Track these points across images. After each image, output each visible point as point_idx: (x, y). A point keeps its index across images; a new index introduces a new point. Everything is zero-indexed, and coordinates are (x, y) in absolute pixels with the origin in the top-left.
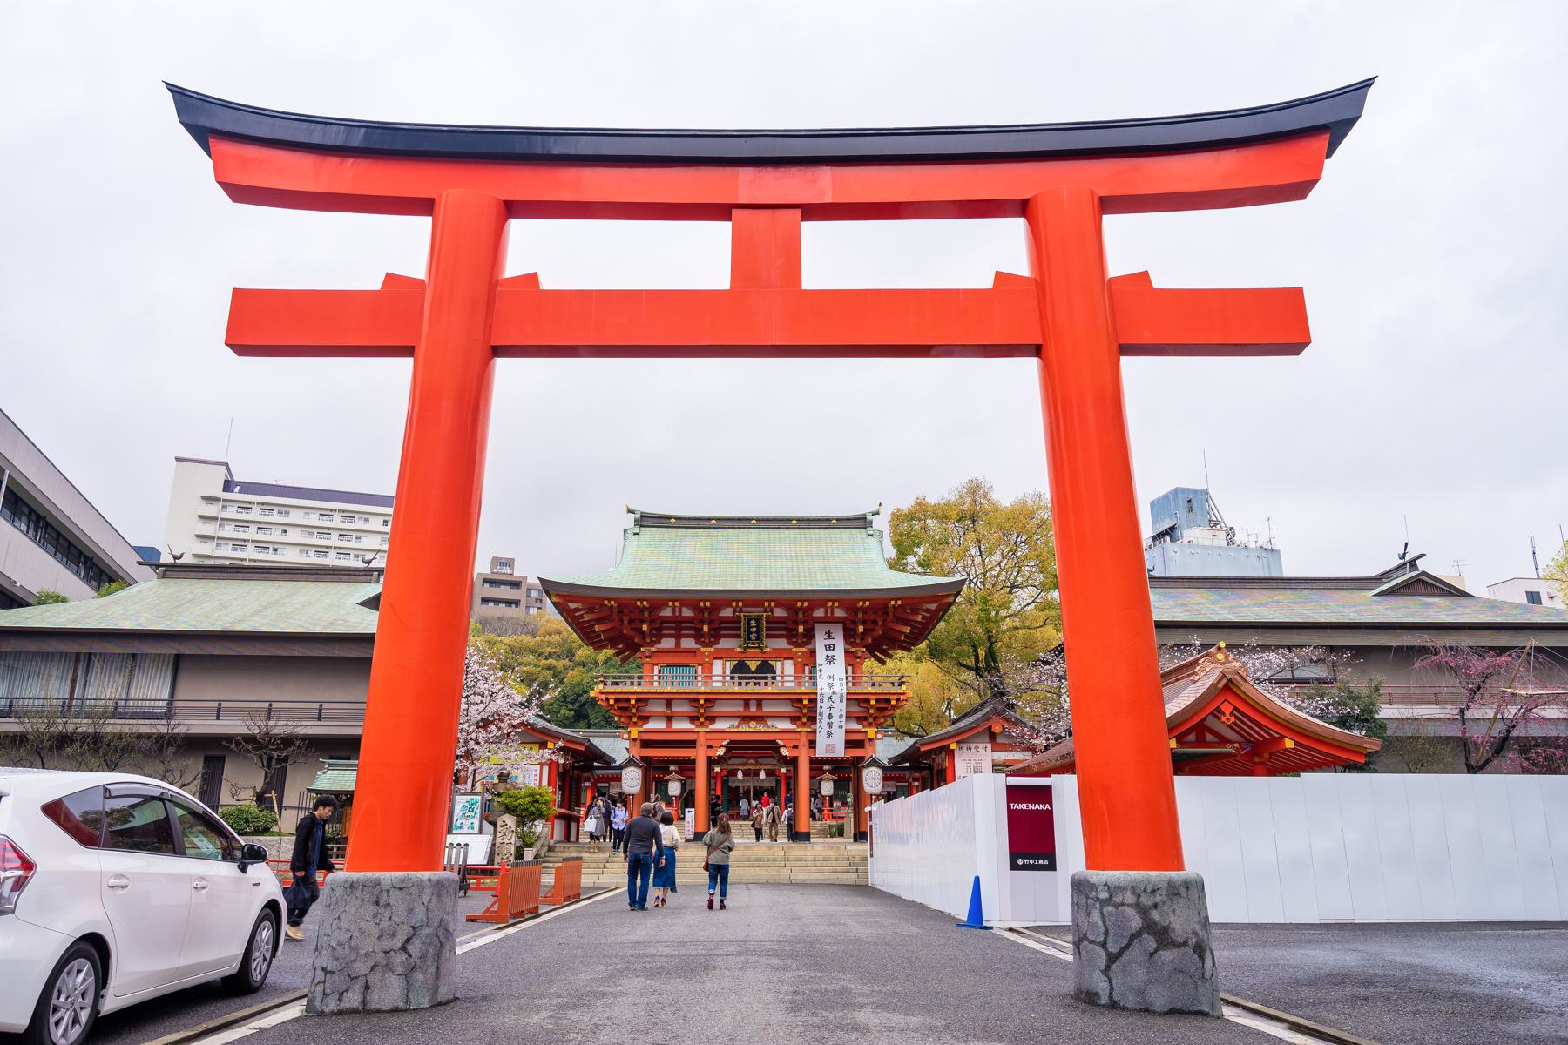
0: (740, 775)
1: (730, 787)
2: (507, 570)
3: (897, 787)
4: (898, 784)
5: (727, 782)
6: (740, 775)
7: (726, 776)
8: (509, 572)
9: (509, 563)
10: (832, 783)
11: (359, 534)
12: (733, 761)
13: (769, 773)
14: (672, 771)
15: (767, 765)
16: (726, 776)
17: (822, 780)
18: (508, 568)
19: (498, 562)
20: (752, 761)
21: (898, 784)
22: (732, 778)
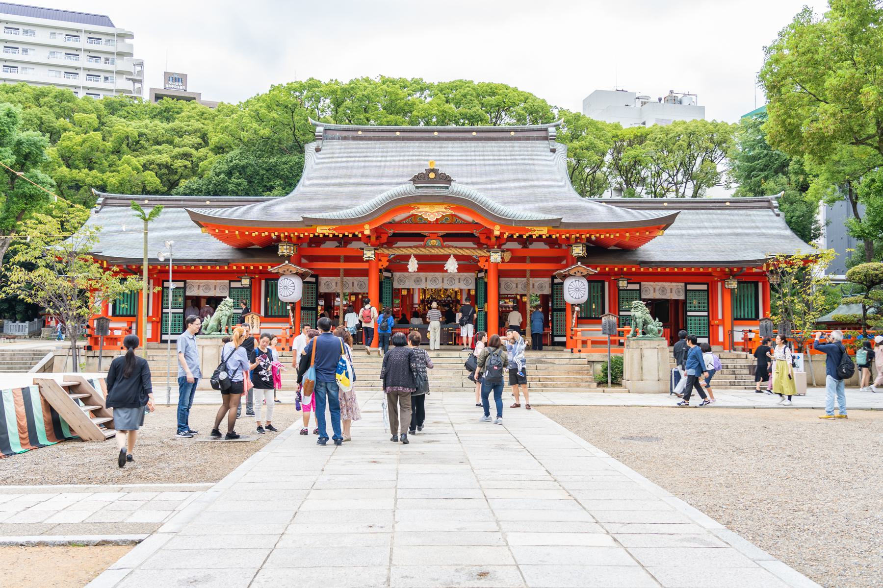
0: (413, 265)
1: (396, 293)
2: (179, 86)
3: (686, 291)
4: (689, 287)
5: (390, 280)
6: (413, 265)
7: (387, 270)
8: (181, 88)
9: (180, 79)
10: (585, 282)
11: (25, 47)
12: (399, 244)
13: (467, 264)
14: (283, 258)
15: (461, 248)
16: (387, 270)
17: (564, 277)
18: (180, 84)
19: (170, 77)
20: (434, 242)
21: (689, 287)
22: (397, 275)
